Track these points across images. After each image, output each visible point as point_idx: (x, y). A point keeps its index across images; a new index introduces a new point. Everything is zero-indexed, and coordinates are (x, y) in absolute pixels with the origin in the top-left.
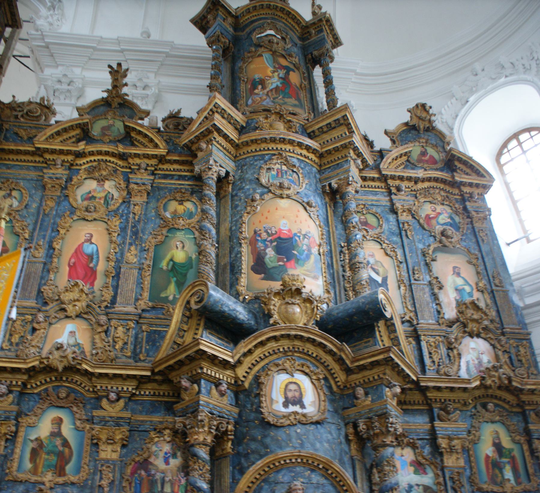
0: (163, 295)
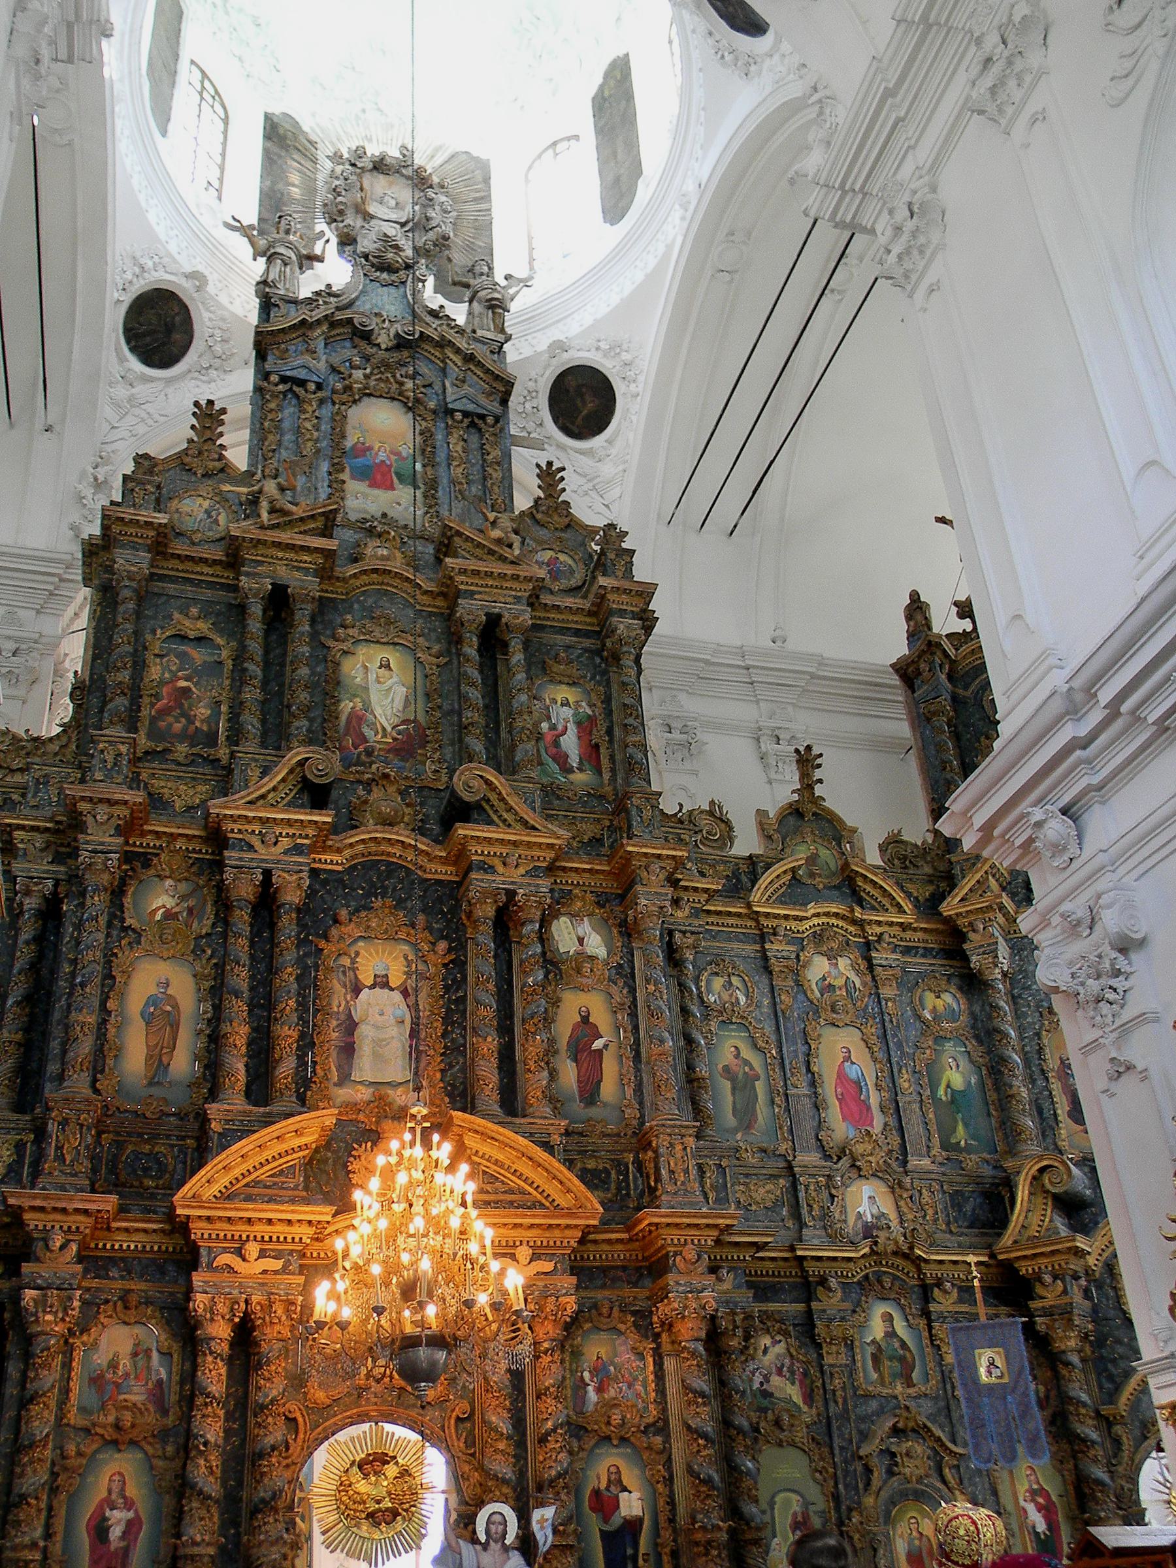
0: (953, 1141)
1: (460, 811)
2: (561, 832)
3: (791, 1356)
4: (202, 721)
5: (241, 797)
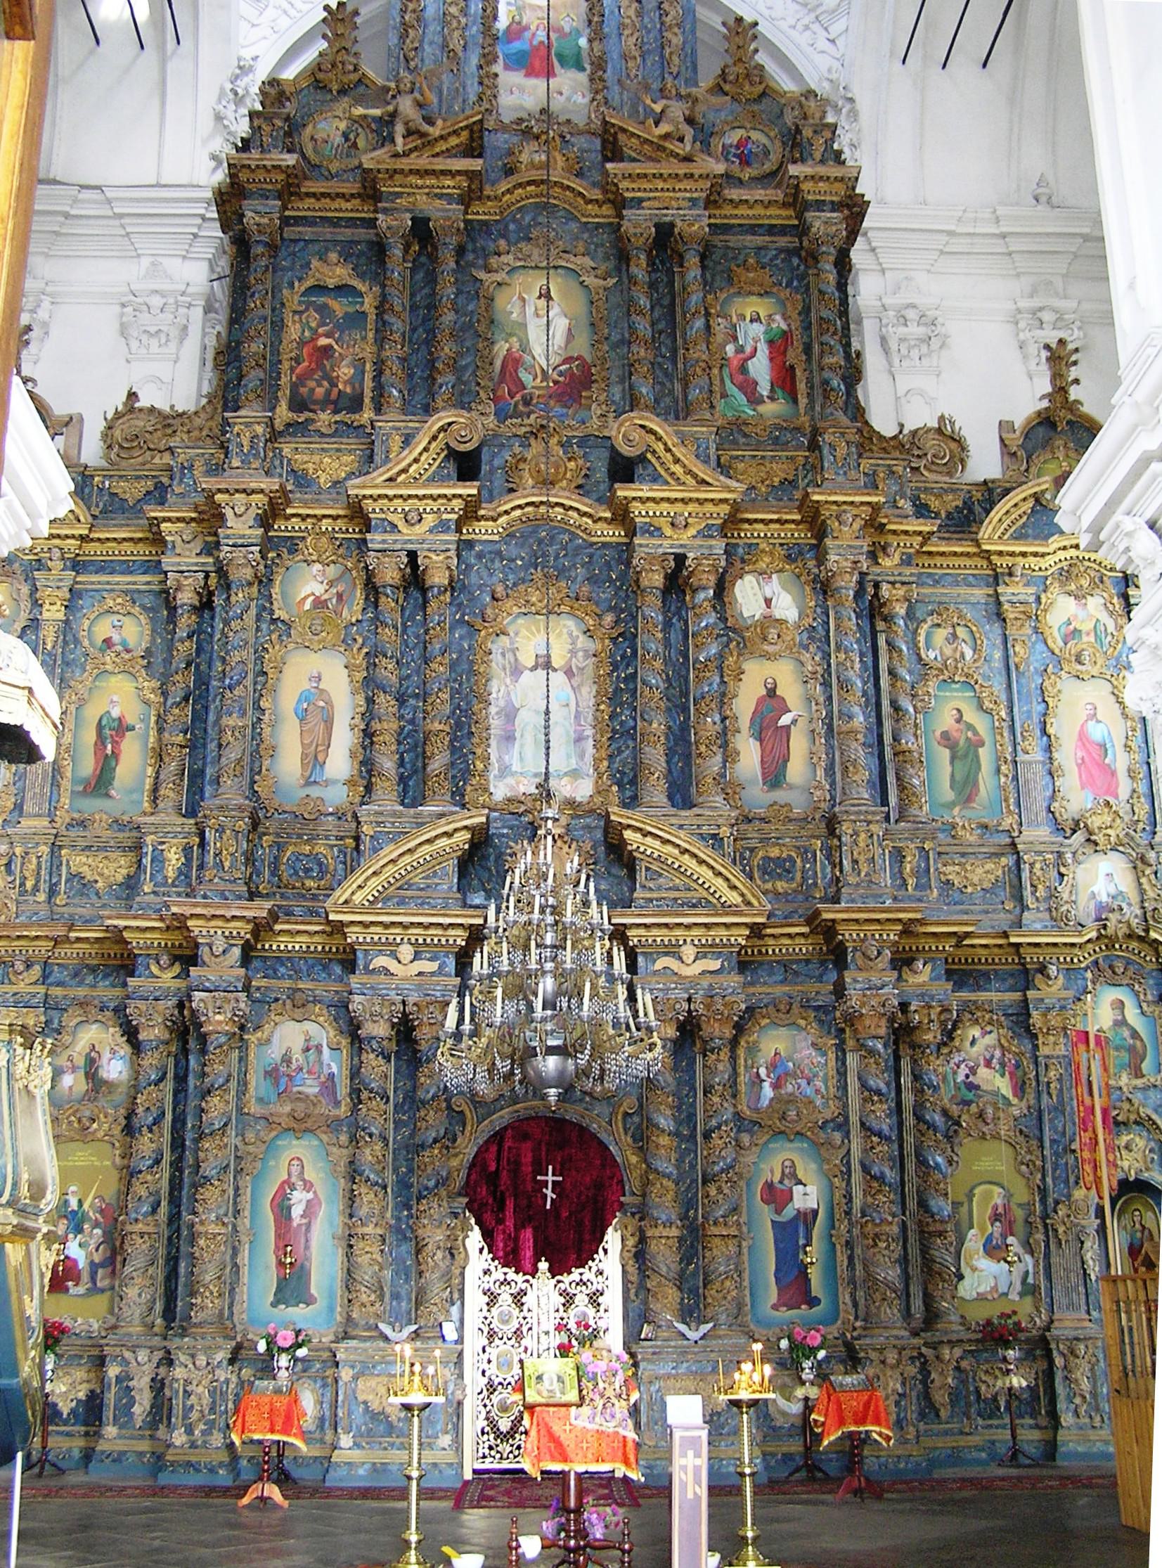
1: (624, 469)
2: (734, 484)
3: (1002, 1046)
4: (345, 383)
5: (379, 476)
